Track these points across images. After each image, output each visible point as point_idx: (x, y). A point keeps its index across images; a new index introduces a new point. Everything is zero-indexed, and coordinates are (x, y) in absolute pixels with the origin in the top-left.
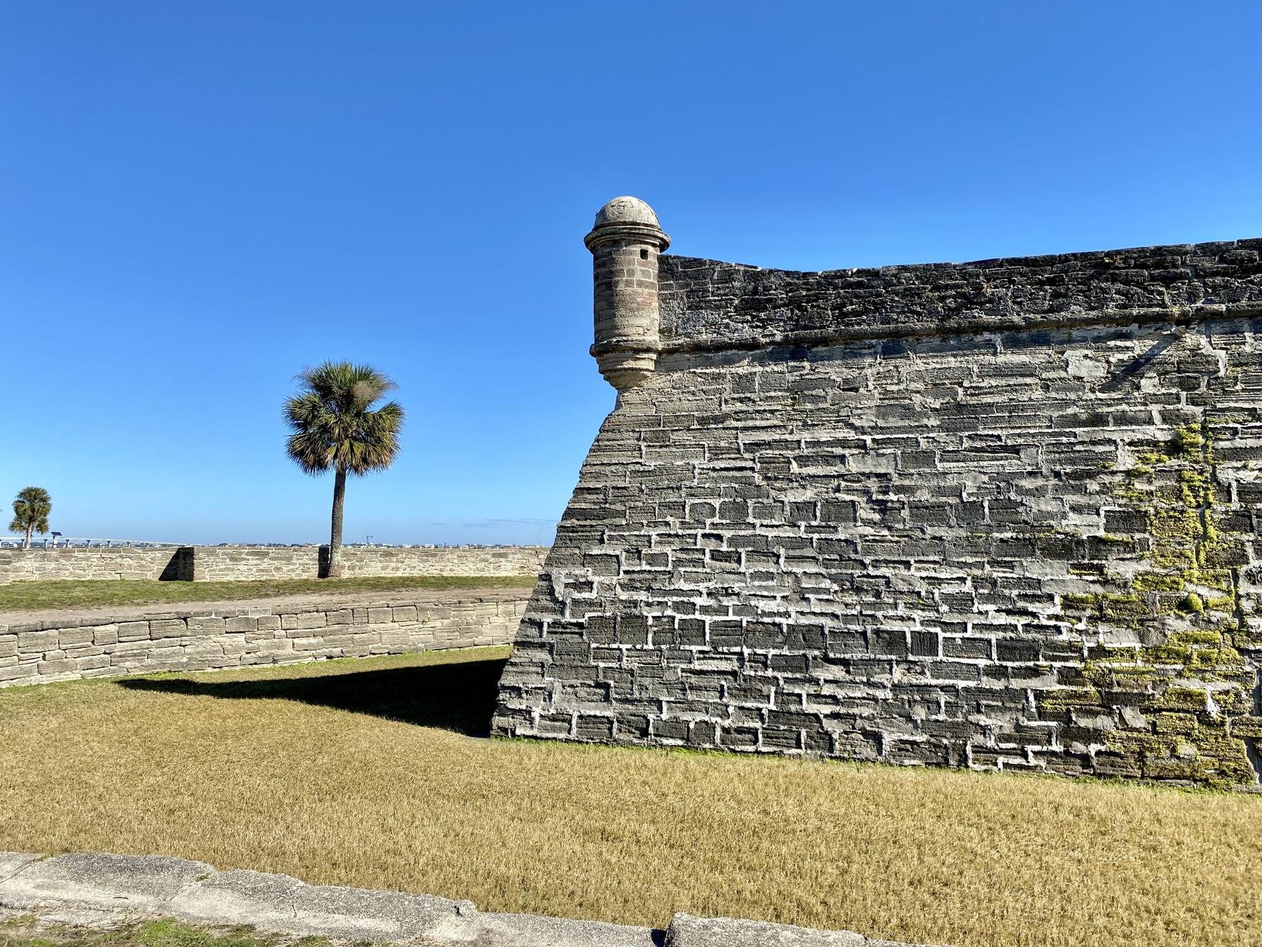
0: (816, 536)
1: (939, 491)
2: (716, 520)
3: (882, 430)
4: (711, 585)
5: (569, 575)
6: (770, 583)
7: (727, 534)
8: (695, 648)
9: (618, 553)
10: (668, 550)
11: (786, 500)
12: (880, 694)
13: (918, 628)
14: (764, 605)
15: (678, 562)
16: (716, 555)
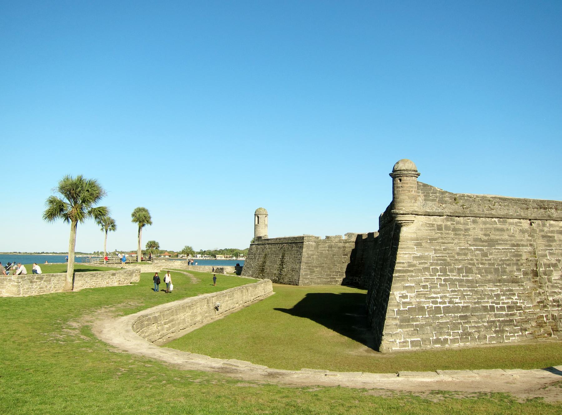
0: (465, 278)
1: (489, 264)
2: (439, 273)
3: (476, 246)
4: (441, 295)
5: (399, 294)
6: (456, 293)
7: (443, 278)
8: (439, 315)
9: (413, 285)
10: (427, 284)
11: (456, 267)
12: (486, 324)
13: (491, 304)
14: (457, 300)
15: (431, 288)
16: (441, 285)
